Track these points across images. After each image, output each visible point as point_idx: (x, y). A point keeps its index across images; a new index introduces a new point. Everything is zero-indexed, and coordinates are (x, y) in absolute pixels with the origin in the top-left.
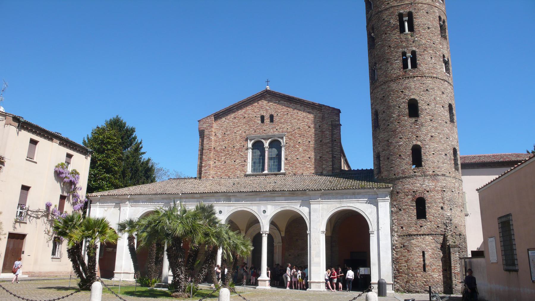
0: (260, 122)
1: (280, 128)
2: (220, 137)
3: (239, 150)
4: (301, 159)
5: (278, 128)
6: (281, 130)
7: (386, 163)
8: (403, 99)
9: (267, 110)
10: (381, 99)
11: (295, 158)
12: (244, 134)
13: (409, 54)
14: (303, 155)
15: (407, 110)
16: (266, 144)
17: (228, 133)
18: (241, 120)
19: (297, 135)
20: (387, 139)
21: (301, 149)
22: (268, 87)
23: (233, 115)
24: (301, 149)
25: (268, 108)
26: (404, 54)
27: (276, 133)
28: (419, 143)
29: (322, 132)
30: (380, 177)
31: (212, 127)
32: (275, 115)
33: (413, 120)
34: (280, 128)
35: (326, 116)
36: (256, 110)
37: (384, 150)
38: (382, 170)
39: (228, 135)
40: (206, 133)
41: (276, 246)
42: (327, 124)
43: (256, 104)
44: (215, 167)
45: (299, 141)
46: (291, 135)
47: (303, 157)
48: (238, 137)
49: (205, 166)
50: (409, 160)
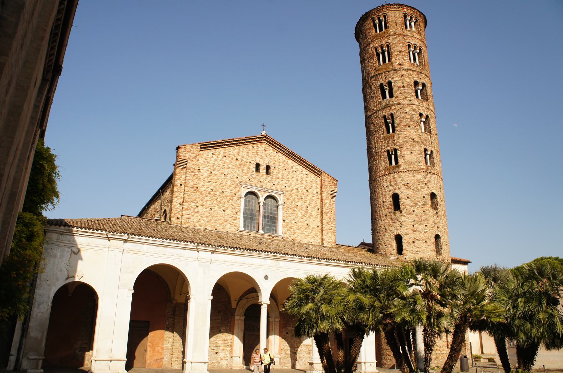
0: (254, 169)
1: (278, 184)
2: (205, 175)
3: (230, 198)
4: (298, 224)
5: (275, 182)
6: (278, 186)
7: (411, 246)
8: (427, 190)
9: (263, 160)
10: (404, 185)
11: (293, 222)
12: (236, 180)
13: (429, 153)
14: (302, 220)
15: (430, 202)
16: (262, 199)
17: (216, 172)
18: (233, 161)
19: (295, 197)
20: (412, 224)
21: (299, 214)
22: (264, 132)
23: (220, 151)
24: (299, 214)
25: (264, 156)
26: (426, 150)
27: (274, 188)
28: (439, 234)
29: (322, 200)
30: (403, 259)
31: (198, 160)
32: (272, 167)
33: (435, 212)
34: (278, 184)
35: (326, 184)
36: (251, 155)
37: (408, 233)
38: (404, 251)
39: (216, 175)
40: (190, 164)
41: (272, 322)
42: (327, 192)
43: (250, 147)
44: (198, 212)
45: (297, 204)
46: (290, 194)
47: (301, 222)
48: (229, 181)
49: (187, 209)
50: (433, 246)
